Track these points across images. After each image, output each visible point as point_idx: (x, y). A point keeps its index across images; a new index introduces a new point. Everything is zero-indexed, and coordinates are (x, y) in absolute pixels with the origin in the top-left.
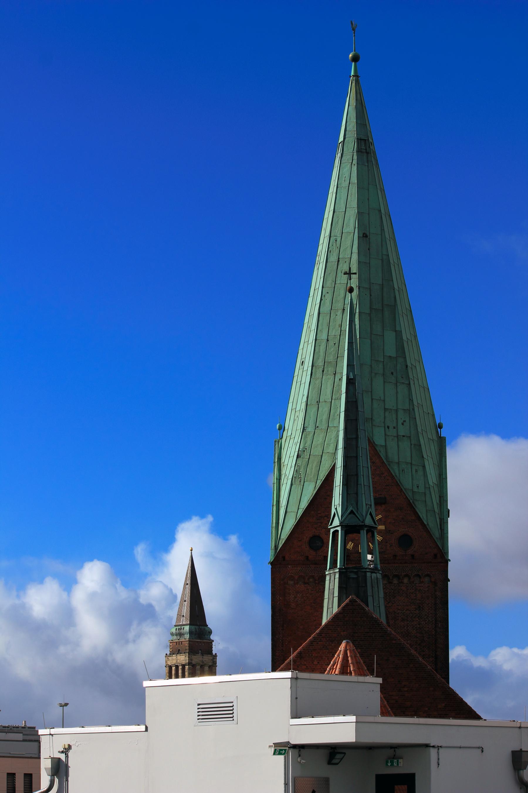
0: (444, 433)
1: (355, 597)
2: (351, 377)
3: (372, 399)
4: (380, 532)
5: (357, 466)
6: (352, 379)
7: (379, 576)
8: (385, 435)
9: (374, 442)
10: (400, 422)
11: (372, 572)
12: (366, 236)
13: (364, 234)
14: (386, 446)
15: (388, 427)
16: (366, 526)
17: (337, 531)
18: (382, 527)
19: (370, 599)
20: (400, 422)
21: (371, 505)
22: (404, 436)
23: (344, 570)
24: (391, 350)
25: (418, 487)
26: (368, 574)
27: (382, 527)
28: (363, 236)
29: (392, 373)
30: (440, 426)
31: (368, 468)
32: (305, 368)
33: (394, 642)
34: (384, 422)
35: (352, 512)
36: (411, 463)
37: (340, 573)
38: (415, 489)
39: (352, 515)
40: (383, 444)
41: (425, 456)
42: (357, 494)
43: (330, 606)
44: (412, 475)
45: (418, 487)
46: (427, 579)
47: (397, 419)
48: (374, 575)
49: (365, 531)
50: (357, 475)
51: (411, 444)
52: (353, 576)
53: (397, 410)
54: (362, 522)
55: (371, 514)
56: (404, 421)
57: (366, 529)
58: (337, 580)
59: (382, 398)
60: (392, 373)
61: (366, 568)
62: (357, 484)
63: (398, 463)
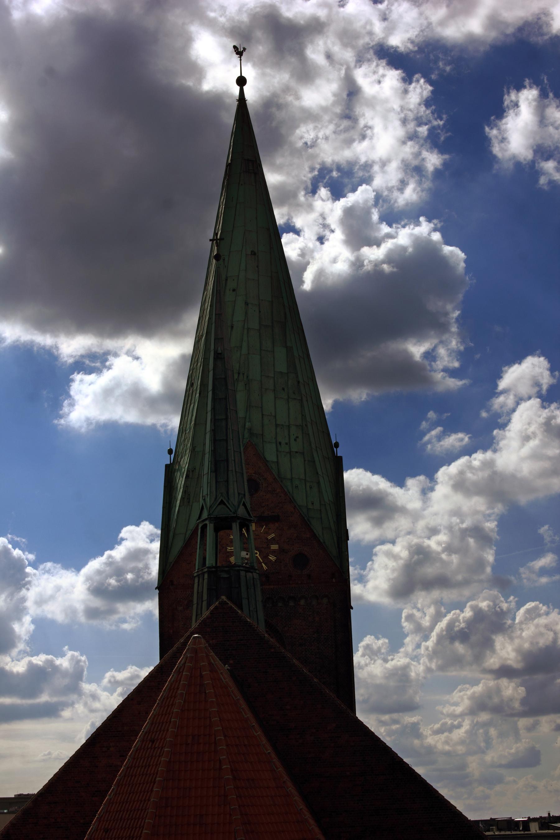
0: (340, 452)
1: (224, 598)
2: (219, 351)
3: (262, 415)
4: (274, 552)
5: (227, 450)
6: (220, 354)
7: (256, 576)
8: (277, 450)
9: (265, 458)
10: (292, 438)
11: (246, 571)
12: (255, 254)
13: (252, 252)
14: (277, 462)
15: (280, 443)
16: (239, 518)
17: (206, 525)
18: (274, 547)
19: (245, 602)
20: (292, 438)
21: (244, 495)
22: (296, 452)
23: (213, 569)
24: (282, 367)
25: (313, 504)
26: (243, 573)
27: (274, 547)
28: (251, 254)
29: (283, 389)
30: (337, 445)
31: (241, 453)
32: (195, 388)
33: (272, 650)
34: (276, 438)
35: (222, 502)
36: (305, 480)
37: (209, 572)
38: (310, 506)
39: (223, 506)
40: (275, 460)
41: (320, 473)
42: (227, 481)
43: (199, 612)
44: (306, 491)
45: (313, 504)
46: (325, 601)
47: (289, 435)
48: (249, 575)
49: (238, 524)
50: (227, 461)
51: (305, 461)
52: (226, 576)
53: (289, 426)
54: (234, 513)
55: (244, 505)
56: (297, 437)
57: (238, 521)
58: (206, 581)
59: (273, 414)
60: (283, 389)
61: (239, 566)
62: (228, 470)
63: (291, 479)
